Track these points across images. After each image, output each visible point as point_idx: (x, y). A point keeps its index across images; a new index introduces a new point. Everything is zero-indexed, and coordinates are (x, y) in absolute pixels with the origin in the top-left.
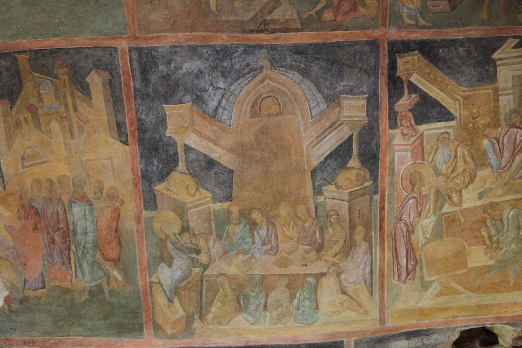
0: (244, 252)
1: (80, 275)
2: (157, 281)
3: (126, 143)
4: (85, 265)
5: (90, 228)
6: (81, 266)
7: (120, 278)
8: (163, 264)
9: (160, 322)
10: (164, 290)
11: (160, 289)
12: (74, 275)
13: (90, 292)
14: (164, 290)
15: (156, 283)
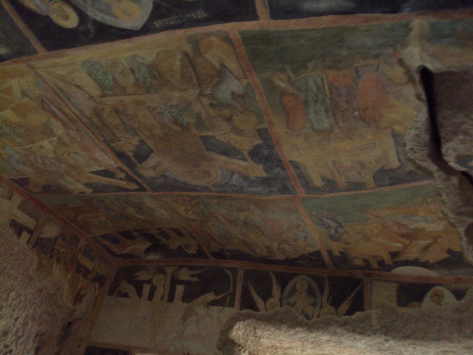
0: (173, 106)
1: (319, 80)
2: (241, 80)
3: (290, 161)
4: (315, 89)
5: (312, 116)
6: (318, 88)
7: (278, 82)
8: (241, 93)
9: (226, 46)
10: (232, 74)
11: (236, 74)
12: (325, 81)
13: (306, 68)
14: (232, 74)
15: (243, 78)
